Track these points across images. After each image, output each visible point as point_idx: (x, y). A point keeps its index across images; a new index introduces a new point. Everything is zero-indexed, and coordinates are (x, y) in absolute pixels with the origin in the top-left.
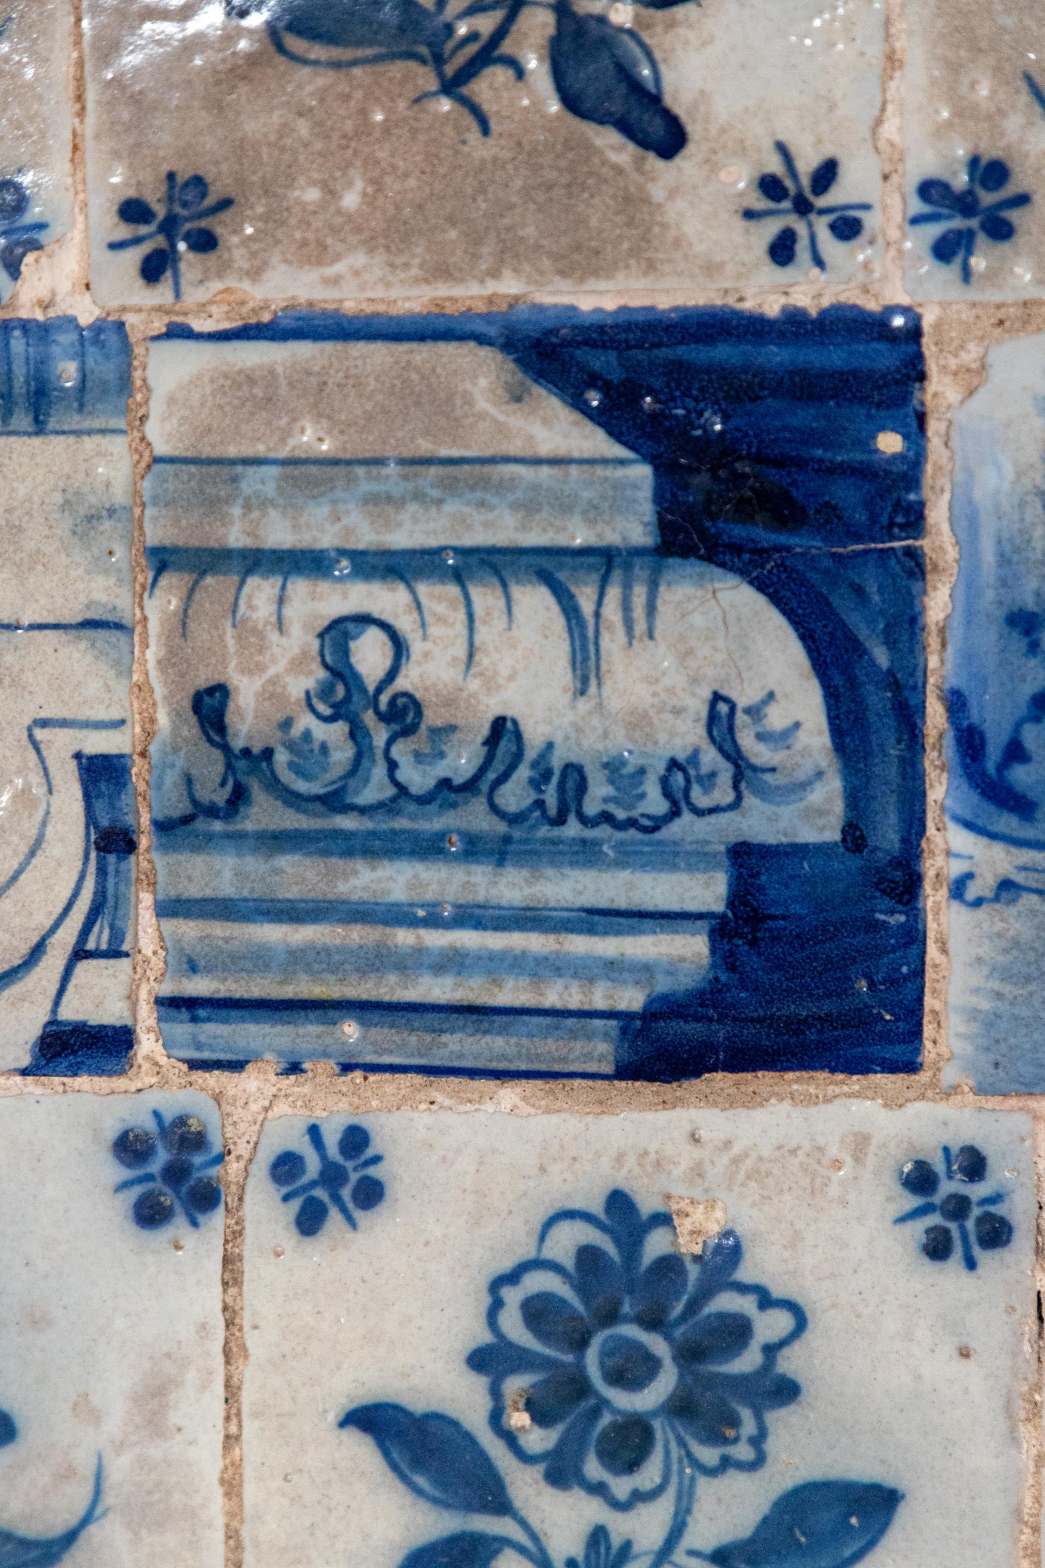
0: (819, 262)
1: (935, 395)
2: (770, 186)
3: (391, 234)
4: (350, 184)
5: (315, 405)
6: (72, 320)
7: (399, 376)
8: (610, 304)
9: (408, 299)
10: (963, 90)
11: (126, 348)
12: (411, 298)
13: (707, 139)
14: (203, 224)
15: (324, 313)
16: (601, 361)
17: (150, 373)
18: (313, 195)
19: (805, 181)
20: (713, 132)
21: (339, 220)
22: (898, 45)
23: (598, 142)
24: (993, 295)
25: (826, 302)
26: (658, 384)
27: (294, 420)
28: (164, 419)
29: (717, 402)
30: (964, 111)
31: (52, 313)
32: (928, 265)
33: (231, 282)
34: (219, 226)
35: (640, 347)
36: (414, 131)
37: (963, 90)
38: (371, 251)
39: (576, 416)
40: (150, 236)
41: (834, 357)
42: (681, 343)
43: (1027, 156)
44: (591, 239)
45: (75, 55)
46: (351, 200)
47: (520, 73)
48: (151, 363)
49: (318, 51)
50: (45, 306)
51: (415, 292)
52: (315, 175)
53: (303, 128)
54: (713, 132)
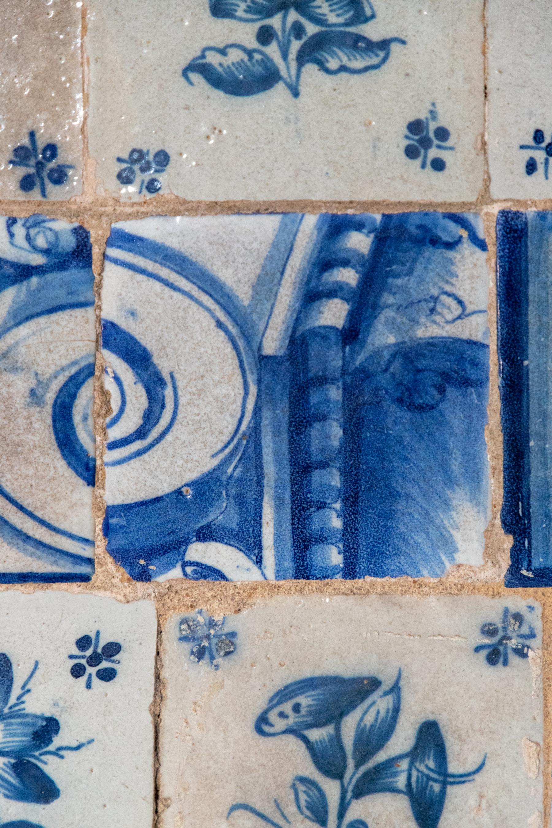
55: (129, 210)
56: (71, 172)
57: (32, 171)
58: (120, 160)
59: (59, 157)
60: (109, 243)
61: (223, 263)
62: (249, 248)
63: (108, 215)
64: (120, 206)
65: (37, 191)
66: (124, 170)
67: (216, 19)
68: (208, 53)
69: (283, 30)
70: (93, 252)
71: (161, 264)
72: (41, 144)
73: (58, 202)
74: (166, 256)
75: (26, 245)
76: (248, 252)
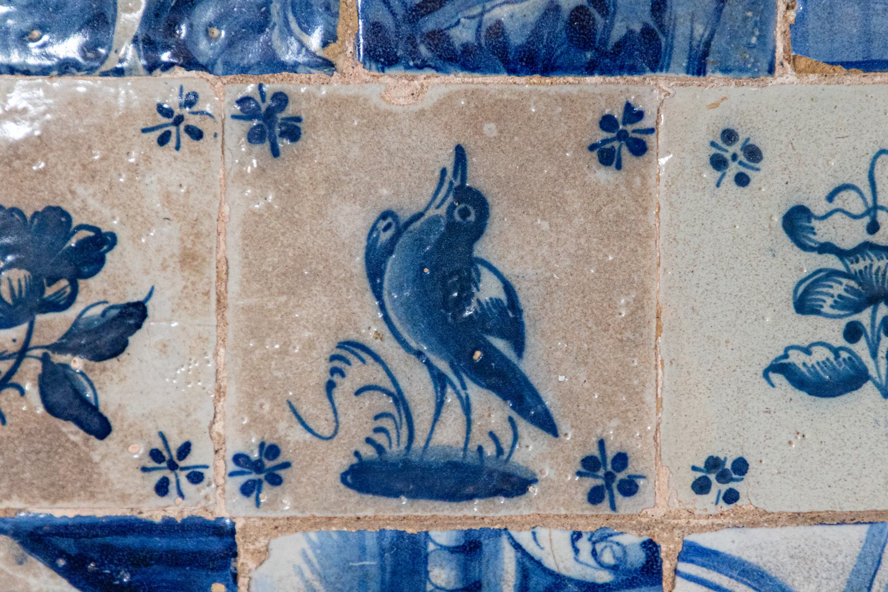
0: (181, 495)
1: (243, 564)
2: (156, 455)
8: (71, 514)
10: (256, 408)
13: (122, 430)
16: (65, 544)
19: (174, 453)
20: (125, 427)
22: (222, 384)
23: (64, 430)
24: (272, 514)
25: (186, 515)
26: (96, 556)
29: (127, 567)
30: (256, 420)
32: (239, 497)
35: (87, 537)
37: (256, 408)
39: (51, 572)
41: (189, 544)
42: (108, 535)
43: (289, 443)
44: (59, 480)
47: (22, 393)
54: (125, 427)
55: (703, 522)
56: (641, 482)
57: (600, 482)
58: (694, 468)
59: (630, 466)
60: (682, 557)
61: (805, 578)
62: (833, 561)
63: (680, 528)
64: (694, 518)
65: (606, 503)
66: (700, 478)
67: (800, 315)
68: (790, 352)
69: (873, 326)
70: (664, 568)
71: (737, 579)
72: (610, 454)
73: (628, 516)
74: (743, 571)
75: (592, 561)
76: (832, 566)
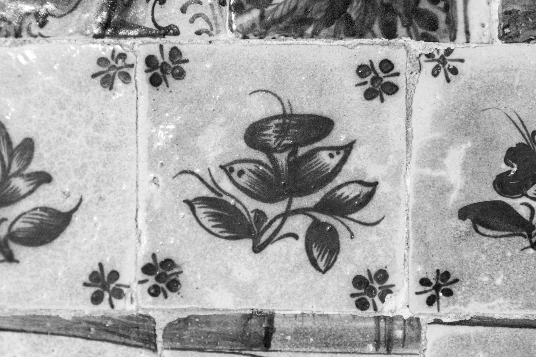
3: (512, 293)
4: (499, 276)
5: (484, 348)
6: (401, 317)
7: (513, 339)
9: (517, 314)
11: (419, 327)
12: (518, 314)
14: (448, 287)
15: (488, 318)
17: (427, 335)
18: (486, 279)
21: (494, 288)
27: (476, 353)
28: (432, 351)
31: (395, 314)
33: (457, 306)
34: (454, 288)
36: (521, 260)
38: (505, 298)
40: (430, 290)
45: (406, 230)
46: (499, 281)
48: (428, 331)
49: (489, 232)
50: (392, 312)
51: (520, 312)
52: (487, 273)
53: (484, 257)
